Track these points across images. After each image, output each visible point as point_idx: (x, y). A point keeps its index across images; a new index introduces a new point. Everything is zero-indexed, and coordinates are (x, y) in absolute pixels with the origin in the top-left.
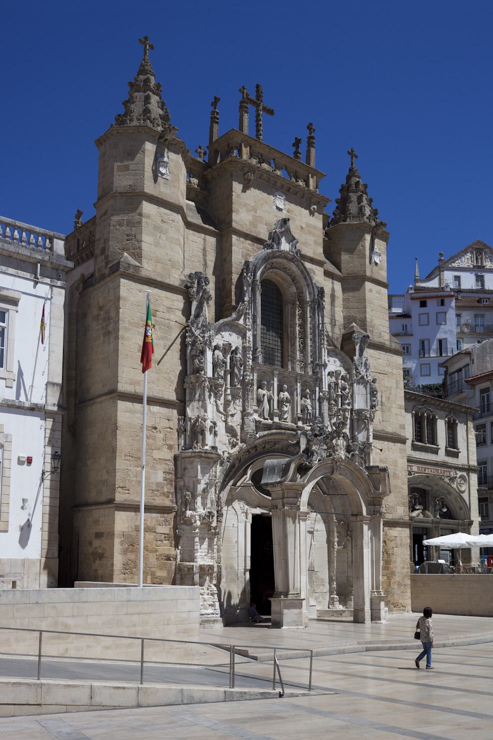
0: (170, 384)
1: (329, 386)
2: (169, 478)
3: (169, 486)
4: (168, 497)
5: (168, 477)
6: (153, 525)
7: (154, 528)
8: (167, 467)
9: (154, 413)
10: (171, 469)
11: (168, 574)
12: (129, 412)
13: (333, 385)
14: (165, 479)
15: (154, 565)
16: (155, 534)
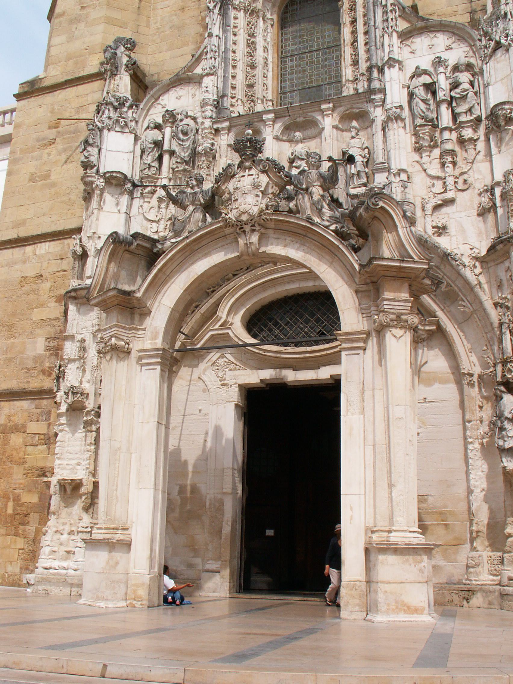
0: (69, 207)
1: (411, 95)
2: (54, 346)
3: (53, 357)
4: (50, 375)
5: (52, 345)
6: (22, 421)
7: (24, 426)
8: (52, 330)
9: (40, 257)
10: (59, 332)
11: (40, 499)
12: (7, 265)
13: (421, 92)
14: (47, 350)
15: (20, 484)
16: (25, 435)
